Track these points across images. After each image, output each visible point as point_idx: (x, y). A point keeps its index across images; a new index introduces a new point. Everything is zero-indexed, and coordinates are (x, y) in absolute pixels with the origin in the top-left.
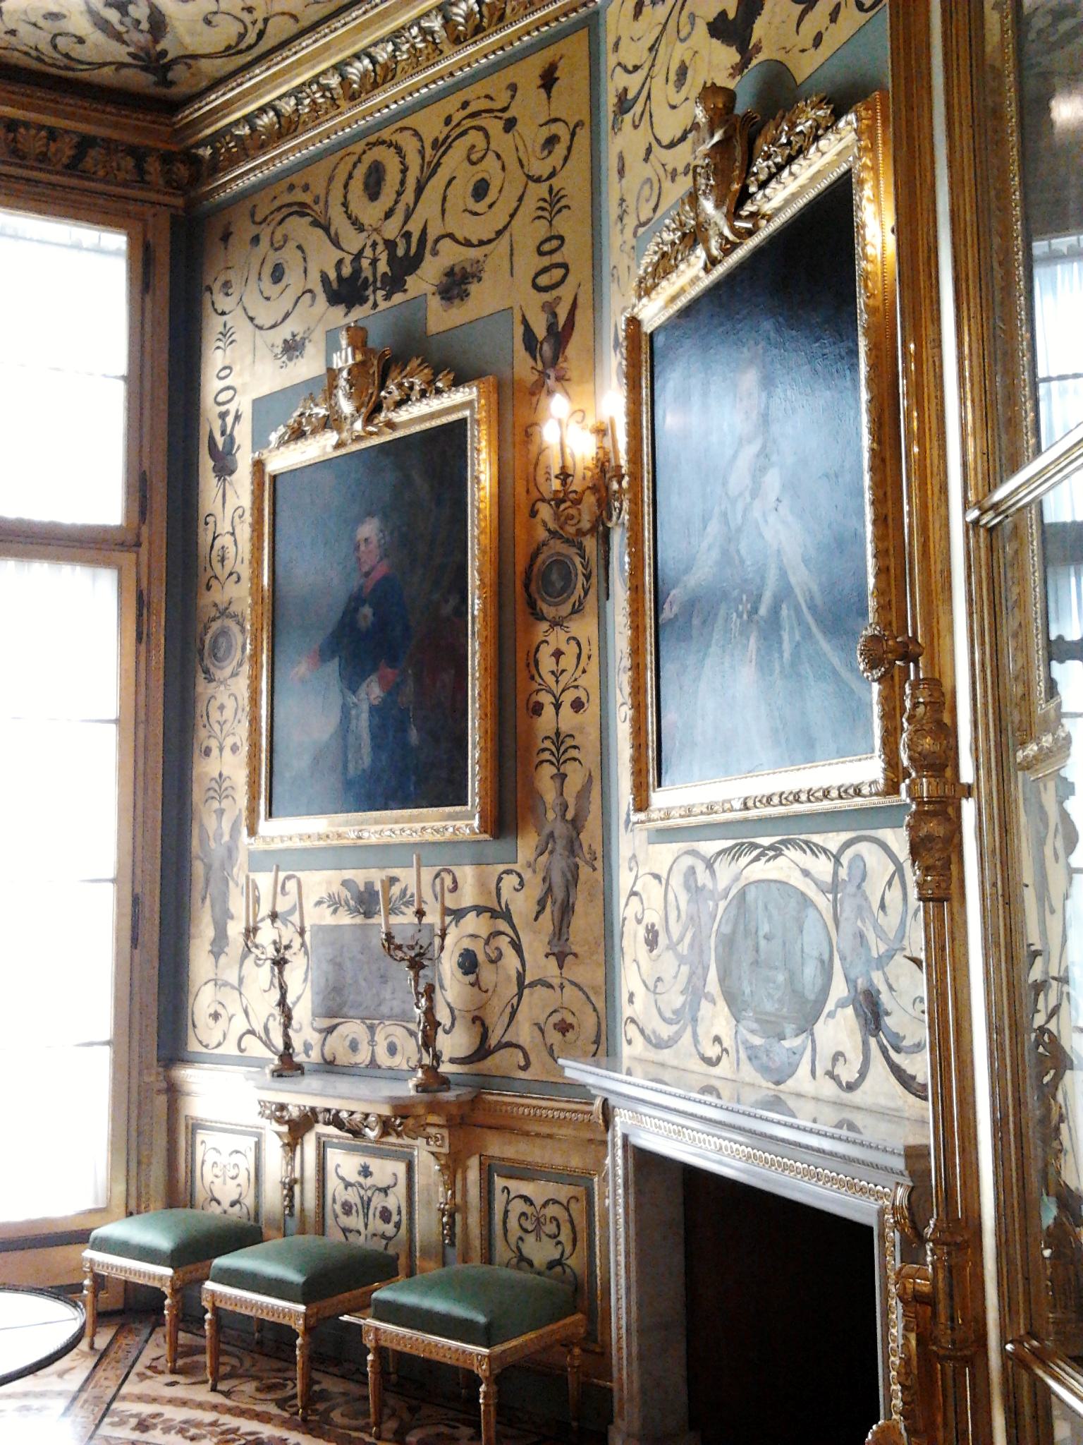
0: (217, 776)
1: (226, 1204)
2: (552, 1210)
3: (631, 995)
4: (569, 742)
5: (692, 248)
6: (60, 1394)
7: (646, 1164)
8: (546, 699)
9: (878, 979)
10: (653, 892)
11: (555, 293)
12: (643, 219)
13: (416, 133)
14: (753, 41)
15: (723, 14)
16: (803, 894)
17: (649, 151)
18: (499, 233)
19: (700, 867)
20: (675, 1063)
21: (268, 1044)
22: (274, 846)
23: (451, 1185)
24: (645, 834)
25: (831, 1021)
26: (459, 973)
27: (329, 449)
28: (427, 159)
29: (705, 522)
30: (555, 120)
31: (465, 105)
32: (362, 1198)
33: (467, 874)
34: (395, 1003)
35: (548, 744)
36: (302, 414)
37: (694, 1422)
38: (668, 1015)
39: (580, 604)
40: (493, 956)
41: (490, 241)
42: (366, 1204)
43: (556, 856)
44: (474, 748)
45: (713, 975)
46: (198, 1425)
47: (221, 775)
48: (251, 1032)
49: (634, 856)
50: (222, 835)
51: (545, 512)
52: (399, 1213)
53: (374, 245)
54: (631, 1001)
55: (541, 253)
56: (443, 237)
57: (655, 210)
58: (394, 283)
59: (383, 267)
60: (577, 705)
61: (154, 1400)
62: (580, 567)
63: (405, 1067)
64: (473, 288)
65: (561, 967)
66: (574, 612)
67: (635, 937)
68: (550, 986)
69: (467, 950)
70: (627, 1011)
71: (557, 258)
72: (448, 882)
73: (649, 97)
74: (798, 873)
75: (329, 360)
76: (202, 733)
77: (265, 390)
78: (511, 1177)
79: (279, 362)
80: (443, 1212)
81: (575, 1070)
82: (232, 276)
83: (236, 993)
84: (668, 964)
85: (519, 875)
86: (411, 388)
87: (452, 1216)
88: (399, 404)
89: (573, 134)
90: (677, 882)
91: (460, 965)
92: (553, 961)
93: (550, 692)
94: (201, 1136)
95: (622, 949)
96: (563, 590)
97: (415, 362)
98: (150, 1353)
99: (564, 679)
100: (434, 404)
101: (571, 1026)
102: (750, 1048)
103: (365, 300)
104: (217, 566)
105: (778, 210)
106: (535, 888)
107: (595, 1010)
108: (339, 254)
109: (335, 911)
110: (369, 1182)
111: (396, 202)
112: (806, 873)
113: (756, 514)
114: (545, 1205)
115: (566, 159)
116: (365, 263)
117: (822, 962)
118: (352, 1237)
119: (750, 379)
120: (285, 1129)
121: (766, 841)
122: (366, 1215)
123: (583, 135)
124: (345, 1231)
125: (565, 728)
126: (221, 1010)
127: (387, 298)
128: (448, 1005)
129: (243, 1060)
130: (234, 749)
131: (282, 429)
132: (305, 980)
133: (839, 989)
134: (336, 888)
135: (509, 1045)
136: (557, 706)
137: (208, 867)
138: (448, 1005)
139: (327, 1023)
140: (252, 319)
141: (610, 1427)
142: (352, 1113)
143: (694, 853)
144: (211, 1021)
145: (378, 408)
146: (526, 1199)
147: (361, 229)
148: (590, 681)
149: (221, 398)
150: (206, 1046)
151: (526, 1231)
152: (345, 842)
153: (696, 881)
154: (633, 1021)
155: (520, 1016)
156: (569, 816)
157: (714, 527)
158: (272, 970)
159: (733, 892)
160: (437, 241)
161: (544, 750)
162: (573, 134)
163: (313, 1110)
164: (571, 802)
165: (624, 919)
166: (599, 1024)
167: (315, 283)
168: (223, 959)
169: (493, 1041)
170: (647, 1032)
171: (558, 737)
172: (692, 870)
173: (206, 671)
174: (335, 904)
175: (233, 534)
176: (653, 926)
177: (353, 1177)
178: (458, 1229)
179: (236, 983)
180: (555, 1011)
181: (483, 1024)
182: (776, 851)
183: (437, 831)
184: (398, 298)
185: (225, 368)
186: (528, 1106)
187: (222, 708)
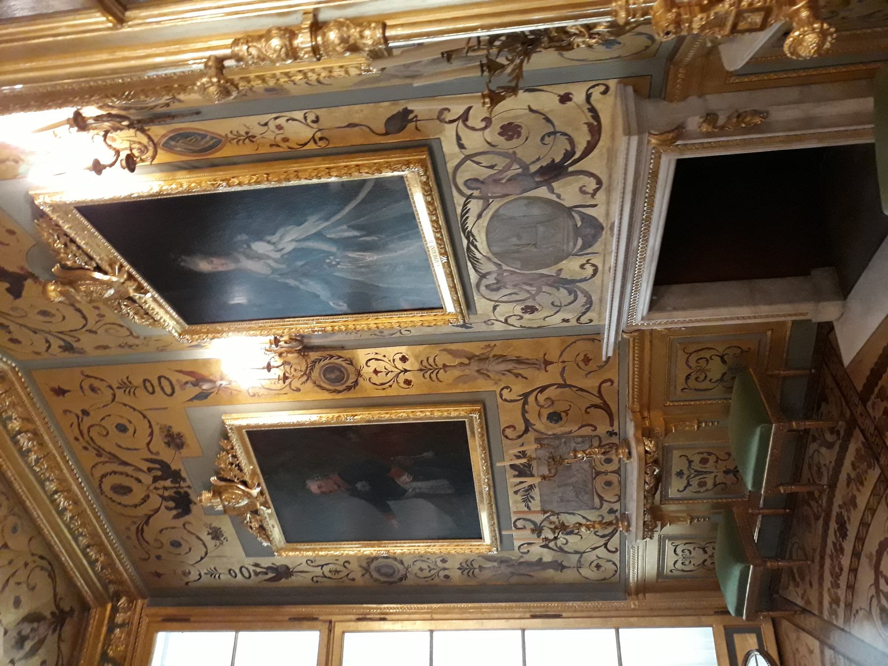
0: (460, 572)
1: (706, 556)
3: (564, 320)
4: (425, 363)
6: (822, 652)
8: (402, 377)
9: (534, 168)
10: (504, 310)
11: (174, 382)
14: (18, 271)
15: (8, 290)
16: (492, 218)
17: (90, 331)
18: (145, 417)
19: (485, 282)
20: (599, 292)
21: (612, 534)
25: (562, 197)
27: (269, 511)
28: (107, 459)
30: (81, 387)
31: (77, 439)
35: (427, 375)
38: (572, 297)
39: (346, 360)
41: (149, 422)
42: (698, 473)
43: (490, 368)
45: (544, 271)
47: (459, 569)
48: (606, 545)
50: (494, 567)
51: (296, 384)
52: (702, 453)
53: (156, 489)
54: (567, 321)
55: (153, 393)
56: (149, 449)
58: (176, 476)
59: (168, 483)
60: (404, 359)
62: (327, 361)
64: (175, 430)
65: (552, 363)
66: (351, 364)
67: (530, 320)
69: (548, 418)
71: (155, 383)
72: (509, 432)
74: (480, 221)
76: (437, 580)
82: (179, 571)
83: (585, 555)
85: (502, 389)
88: (241, 470)
90: (496, 296)
91: (557, 422)
92: (549, 368)
96: (341, 372)
99: (390, 368)
100: (239, 451)
101: (585, 356)
102: (583, 247)
103: (186, 493)
107: (575, 342)
108: (163, 507)
110: (686, 472)
111: (132, 477)
112: (479, 216)
114: (690, 367)
116: (166, 494)
121: (465, 242)
122: (705, 473)
123: (88, 371)
124: (715, 485)
125: (417, 366)
126: (594, 564)
127: (184, 480)
128: (580, 428)
129: (621, 550)
131: (259, 539)
132: (573, 514)
133: (542, 192)
135: (599, 391)
136: (406, 371)
137: (513, 574)
138: (580, 428)
139: (597, 500)
140: (202, 558)
141: (814, 320)
142: (645, 482)
143: (478, 285)
144: (602, 569)
146: (688, 377)
149: (247, 575)
150: (616, 571)
151: (706, 377)
154: (578, 319)
158: (567, 534)
159: (496, 260)
160: (151, 453)
162: (88, 376)
165: (521, 326)
168: (564, 563)
169: (598, 401)
172: (487, 287)
173: (401, 579)
175: (322, 566)
176: (522, 309)
177: (685, 482)
179: (578, 556)
180: (578, 365)
182: (469, 235)
184: (184, 474)
185: (230, 573)
186: (633, 379)
187: (421, 569)
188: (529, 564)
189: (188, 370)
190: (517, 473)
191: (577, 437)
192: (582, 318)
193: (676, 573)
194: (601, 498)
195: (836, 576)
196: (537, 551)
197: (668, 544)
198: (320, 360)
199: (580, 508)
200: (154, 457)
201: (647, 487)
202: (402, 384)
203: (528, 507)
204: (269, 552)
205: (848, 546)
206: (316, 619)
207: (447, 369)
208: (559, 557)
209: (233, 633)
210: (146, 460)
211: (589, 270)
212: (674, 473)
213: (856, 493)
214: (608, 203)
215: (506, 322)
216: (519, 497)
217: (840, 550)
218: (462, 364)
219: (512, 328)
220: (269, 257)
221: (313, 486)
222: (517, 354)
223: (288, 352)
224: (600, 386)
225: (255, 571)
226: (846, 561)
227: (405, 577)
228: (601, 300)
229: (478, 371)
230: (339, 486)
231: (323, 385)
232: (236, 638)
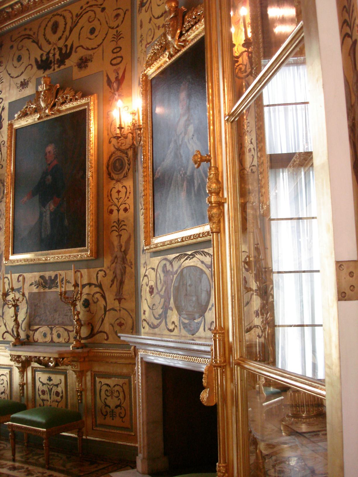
2: (117, 388)
3: (145, 311)
4: (123, 223)
5: (164, 51)
7: (150, 367)
8: (114, 208)
11: (118, 66)
12: (148, 42)
13: (70, 12)
16: (201, 269)
17: (151, 19)
18: (99, 46)
19: (168, 264)
20: (159, 333)
21: (13, 336)
22: (14, 264)
23: (80, 381)
24: (149, 254)
26: (83, 308)
27: (36, 120)
28: (74, 20)
29: (169, 143)
31: (88, 3)
32: (48, 389)
34: (60, 319)
36: (27, 107)
37: (165, 454)
38: (157, 316)
40: (96, 300)
41: (95, 48)
42: (50, 390)
44: (88, 226)
49: (145, 262)
52: (62, 393)
53: (54, 49)
54: (144, 314)
56: (79, 46)
57: (152, 39)
58: (61, 62)
59: (57, 57)
60: (126, 210)
62: (126, 161)
63: (64, 342)
64: (89, 64)
65: (120, 303)
66: (125, 177)
67: (146, 290)
68: (116, 310)
70: (143, 317)
71: (119, 54)
73: (151, 2)
74: (200, 263)
75: (37, 88)
77: (13, 99)
78: (103, 378)
79: (19, 89)
80: (78, 391)
81: (125, 337)
83: (1, 318)
85: (105, 271)
86: (67, 98)
87: (81, 392)
88: (62, 104)
89: (125, 13)
90: (160, 270)
92: (117, 302)
93: (116, 205)
97: (68, 89)
100: (75, 104)
101: (123, 324)
102: (184, 324)
103: (50, 68)
105: (192, 40)
106: (110, 277)
108: (42, 52)
109: (37, 287)
110: (51, 383)
111: (63, 35)
112: (202, 262)
113: (186, 140)
114: (115, 386)
115: (122, 22)
116: (51, 55)
117: (207, 291)
118: (45, 402)
119: (183, 95)
120: (20, 365)
122: (50, 394)
123: (128, 14)
124: (43, 400)
125: (121, 218)
127: (59, 67)
131: (19, 113)
134: (37, 279)
135: (101, 332)
136: (118, 210)
140: (9, 74)
141: (137, 457)
142: (45, 357)
143: (166, 259)
145: (54, 105)
146: (108, 385)
147: (50, 43)
148: (130, 201)
151: (108, 396)
152: (41, 262)
153: (166, 269)
155: (105, 321)
157: (172, 145)
159: (179, 271)
160: (77, 48)
161: (114, 226)
162: (125, 13)
163: (30, 357)
164: (123, 244)
166: (133, 323)
167: (33, 63)
169: (96, 331)
170: (150, 323)
171: (119, 221)
172: (165, 265)
174: (38, 284)
176: (152, 286)
178: (84, 397)
180: (118, 319)
181: (92, 325)
183: (75, 256)
184: (62, 67)
189: (126, 75)
190: (53, 278)
197: (7, 371)
200: (74, 49)
201: (42, 358)
202: (110, 208)
207: (119, 237)
210: (72, 45)
211: (171, 327)
214: (205, 338)
215: (145, 276)
219: (142, 279)
220: (185, 134)
221: (50, 148)
222: (126, 281)
224: (104, 332)
228: (155, 334)
229: (116, 257)
230: (49, 164)
231: (113, 158)
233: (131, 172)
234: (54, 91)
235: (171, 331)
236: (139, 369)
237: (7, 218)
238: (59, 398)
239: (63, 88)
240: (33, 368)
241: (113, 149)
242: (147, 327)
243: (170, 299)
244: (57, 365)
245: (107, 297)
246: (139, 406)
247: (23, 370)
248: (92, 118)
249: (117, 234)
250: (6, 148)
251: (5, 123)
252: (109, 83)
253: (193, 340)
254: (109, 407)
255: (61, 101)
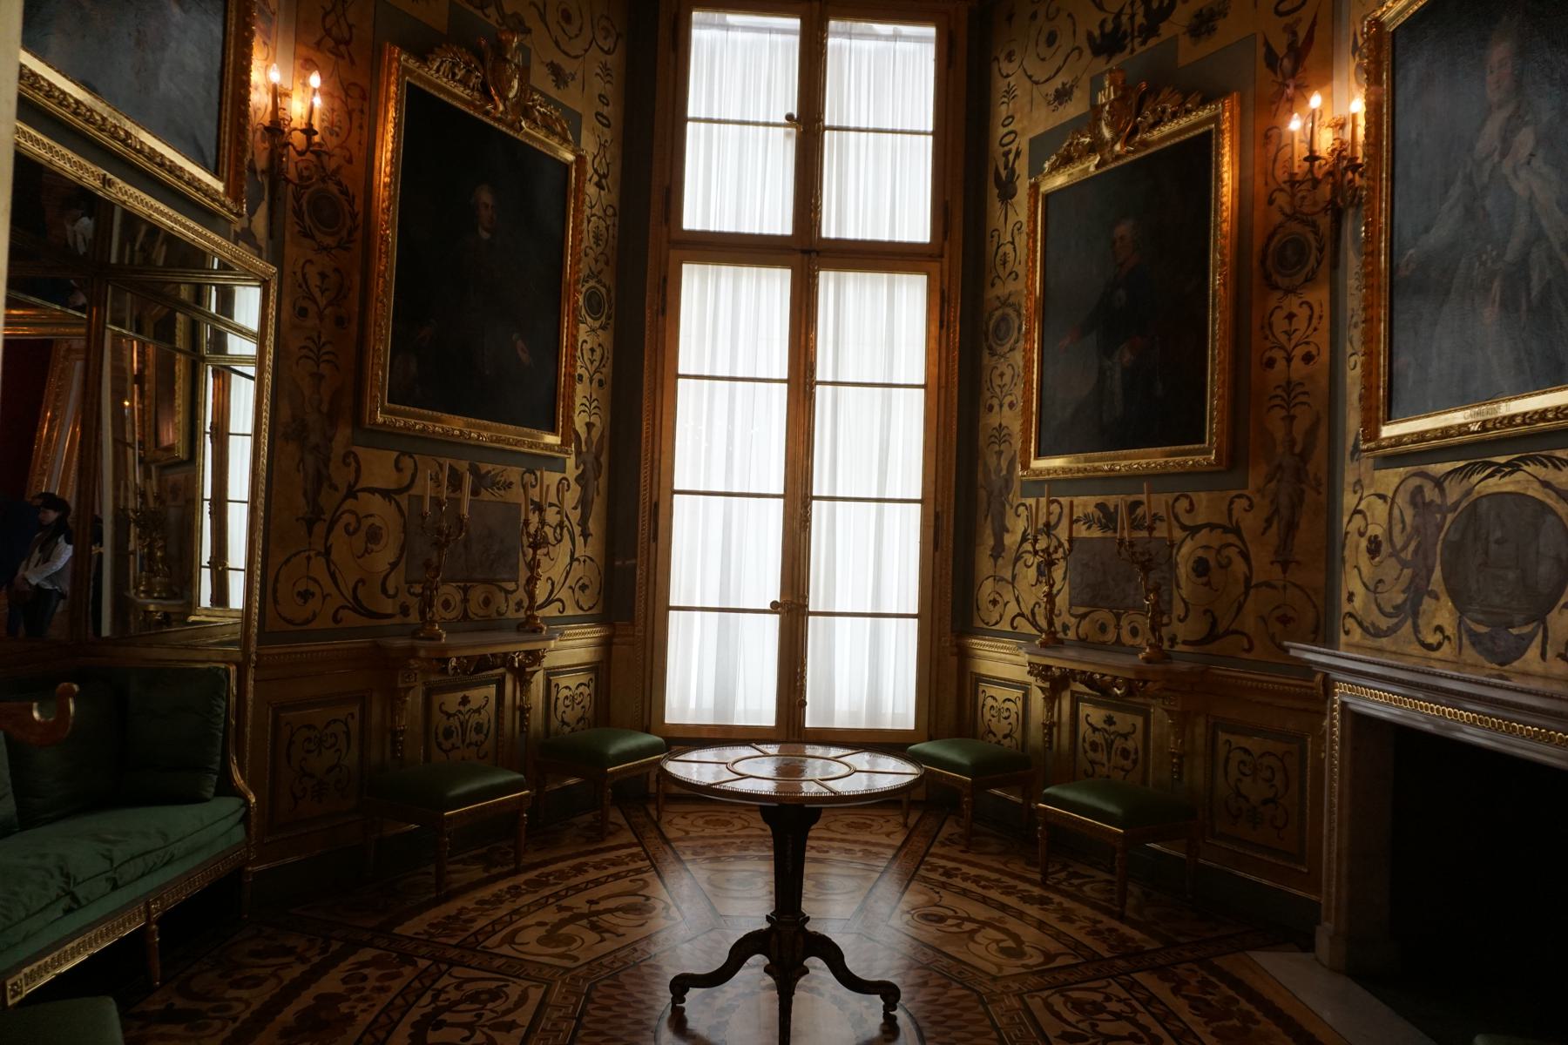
1: (1000, 736)
3: (1351, 596)
4: (1299, 389)
6: (889, 846)
8: (1279, 355)
11: (1296, 15)
16: (1541, 503)
21: (1035, 624)
24: (1371, 461)
27: (1092, 169)
33: (1202, 498)
35: (1279, 392)
38: (1389, 609)
40: (1224, 562)
42: (1110, 745)
45: (1437, 574)
46: (987, 879)
48: (1021, 615)
51: (1282, 199)
58: (1150, 30)
59: (1140, 19)
60: (1308, 358)
61: (954, 860)
62: (1314, 244)
64: (1220, 24)
65: (1284, 572)
66: (1306, 281)
67: (1357, 547)
68: (1274, 587)
70: (1346, 608)
72: (1183, 504)
74: (1537, 485)
75: (1093, 98)
77: (1040, 130)
78: (1233, 733)
84: (1390, 569)
85: (1249, 499)
86: (1164, 111)
92: (1277, 568)
93: (1282, 348)
94: (983, 686)
95: (1343, 559)
97: (1166, 91)
98: (948, 829)
99: (1296, 337)
100: (1184, 122)
103: (1123, 48)
104: (1000, 269)
108: (1102, 16)
110: (1113, 728)
113: (1506, 168)
116: (1125, 19)
120: (1047, 685)
121: (1502, 460)
124: (1092, 762)
125: (1295, 377)
127: (1144, 43)
129: (1014, 634)
130: (1011, 405)
135: (1236, 632)
136: (1289, 360)
137: (990, 494)
139: (1082, 610)
140: (1030, 77)
141: (1318, 928)
145: (1134, 132)
146: (1246, 751)
148: (1322, 338)
149: (1006, 140)
153: (1423, 497)
154: (1351, 615)
156: (1297, 450)
159: (1464, 504)
164: (1299, 438)
168: (1000, 561)
169: (1221, 629)
171: (1289, 385)
172: (1419, 490)
173: (990, 348)
177: (1100, 725)
182: (1514, 467)
184: (1152, 42)
187: (1002, 375)
188: (1002, 515)
189: (1317, 34)
191: (1171, 595)
192: (1351, 620)
193: (981, 697)
194: (1084, 616)
195: (976, 880)
196: (1018, 526)
197: (1016, 694)
198: (1316, 233)
199: (1072, 588)
202: (1268, 354)
203: (1078, 520)
204: (1035, 170)
205: (1011, 901)
206: (945, 238)
208: (1009, 555)
209: (930, 128)
211: (1432, 639)
212: (1112, 713)
213: (1079, 924)
214: (1546, 677)
216: (1091, 509)
217: (1008, 891)
218: (1293, 443)
219: (1346, 519)
220: (1503, 155)
221: (1124, 229)
223: (1333, 185)
224: (1243, 634)
225: (1009, 152)
226: (994, 894)
227: (993, 354)
228: (1380, 650)
229: (1280, 467)
232: (925, 133)
233: (1325, 268)
234: (1133, 100)
235: (1429, 647)
236: (1334, 724)
237: (1028, 383)
238: (1127, 764)
239: (1154, 91)
240: (1073, 693)
241: (1278, 218)
242: (1357, 634)
243: (1431, 571)
244: (1130, 692)
245: (1252, 556)
246: (1331, 812)
247: (1052, 696)
248: (1226, 150)
249: (1283, 413)
250: (1024, 237)
251: (1023, 185)
252: (1272, 61)
253: (1501, 677)
254: (1246, 799)
255: (1151, 120)
